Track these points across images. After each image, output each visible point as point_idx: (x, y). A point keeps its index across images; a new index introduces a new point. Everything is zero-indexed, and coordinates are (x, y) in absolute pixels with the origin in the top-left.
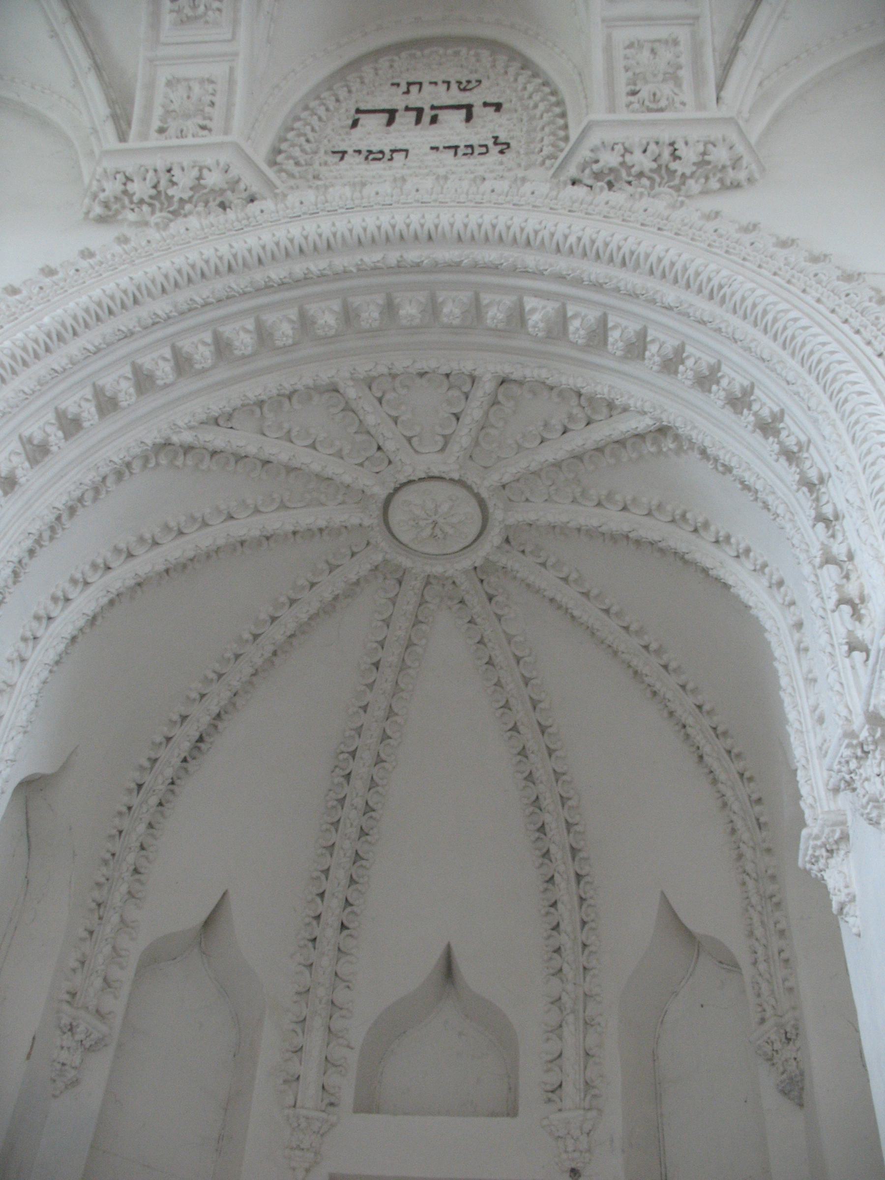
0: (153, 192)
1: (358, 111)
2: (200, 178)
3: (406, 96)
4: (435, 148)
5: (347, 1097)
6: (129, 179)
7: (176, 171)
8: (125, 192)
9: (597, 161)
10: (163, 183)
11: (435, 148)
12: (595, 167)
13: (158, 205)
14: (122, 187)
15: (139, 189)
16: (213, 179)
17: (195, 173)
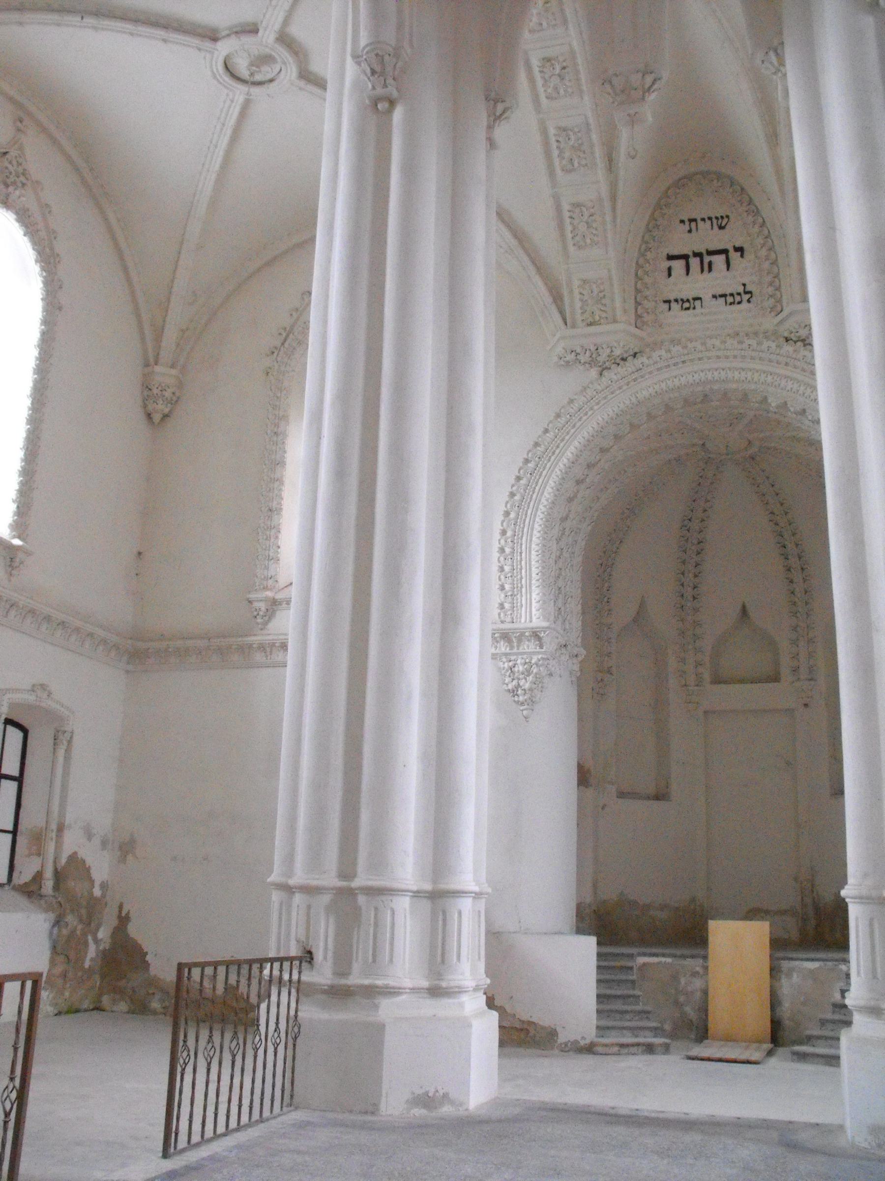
0: (590, 359)
1: (670, 258)
2: (612, 351)
3: (689, 234)
4: (714, 297)
5: (707, 676)
6: (577, 354)
7: (600, 350)
8: (577, 359)
9: (797, 332)
10: (594, 356)
11: (714, 297)
12: (798, 334)
13: (593, 363)
14: (575, 358)
15: (582, 358)
16: (618, 352)
17: (608, 351)
